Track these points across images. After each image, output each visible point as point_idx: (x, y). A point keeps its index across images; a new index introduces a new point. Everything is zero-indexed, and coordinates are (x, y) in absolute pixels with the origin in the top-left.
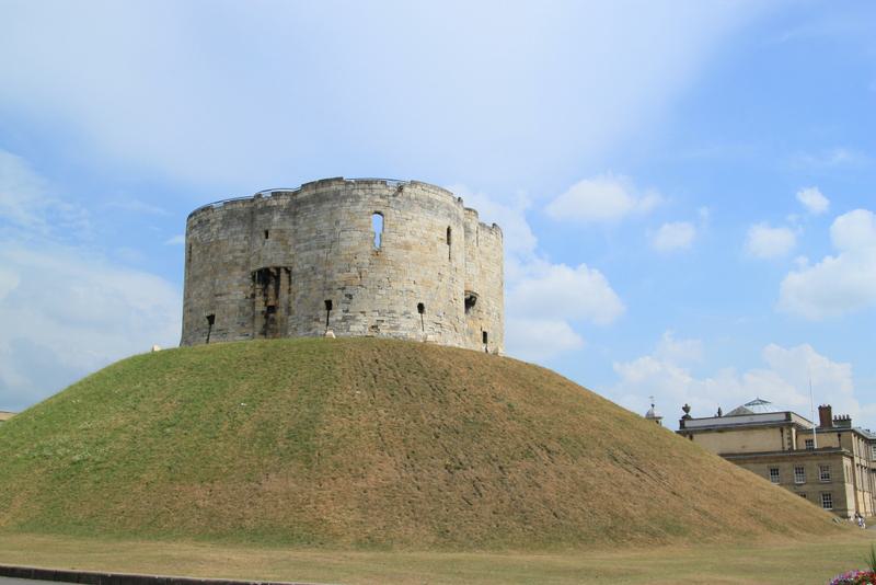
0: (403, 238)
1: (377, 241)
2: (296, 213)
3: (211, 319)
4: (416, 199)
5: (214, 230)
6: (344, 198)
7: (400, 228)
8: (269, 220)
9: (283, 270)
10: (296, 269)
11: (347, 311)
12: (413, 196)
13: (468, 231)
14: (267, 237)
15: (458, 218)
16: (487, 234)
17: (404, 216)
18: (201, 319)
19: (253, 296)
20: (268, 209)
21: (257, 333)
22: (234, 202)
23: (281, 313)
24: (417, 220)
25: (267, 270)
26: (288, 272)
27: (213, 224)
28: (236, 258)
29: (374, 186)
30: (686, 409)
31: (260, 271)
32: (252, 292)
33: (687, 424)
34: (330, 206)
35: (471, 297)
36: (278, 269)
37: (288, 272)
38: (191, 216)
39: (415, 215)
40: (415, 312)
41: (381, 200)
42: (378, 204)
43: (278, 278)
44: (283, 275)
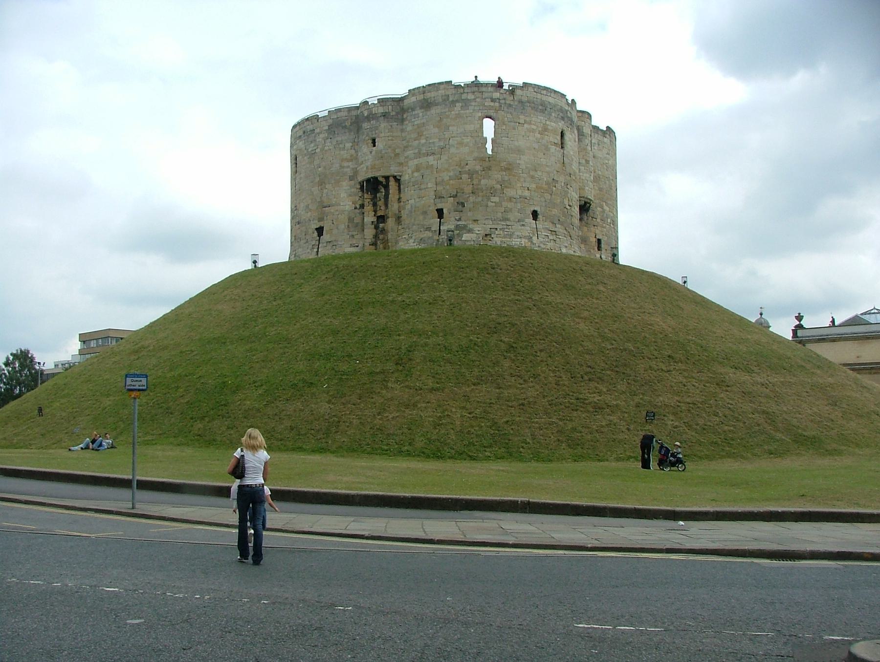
1: (489, 146)
2: (403, 121)
3: (320, 231)
4: (529, 102)
5: (319, 139)
6: (454, 102)
8: (377, 128)
9: (391, 179)
10: (405, 178)
11: (460, 220)
12: (525, 99)
13: (581, 134)
14: (374, 146)
15: (572, 121)
16: (600, 137)
18: (310, 231)
19: (362, 206)
20: (371, 117)
21: (367, 244)
22: (338, 110)
23: (391, 223)
24: (530, 124)
25: (375, 179)
27: (319, 134)
29: (484, 89)
30: (799, 318)
31: (368, 180)
32: (360, 202)
33: (800, 333)
34: (438, 111)
35: (586, 203)
36: (387, 178)
37: (397, 180)
38: (295, 127)
40: (530, 220)
41: (492, 104)
43: (386, 187)
44: (392, 183)
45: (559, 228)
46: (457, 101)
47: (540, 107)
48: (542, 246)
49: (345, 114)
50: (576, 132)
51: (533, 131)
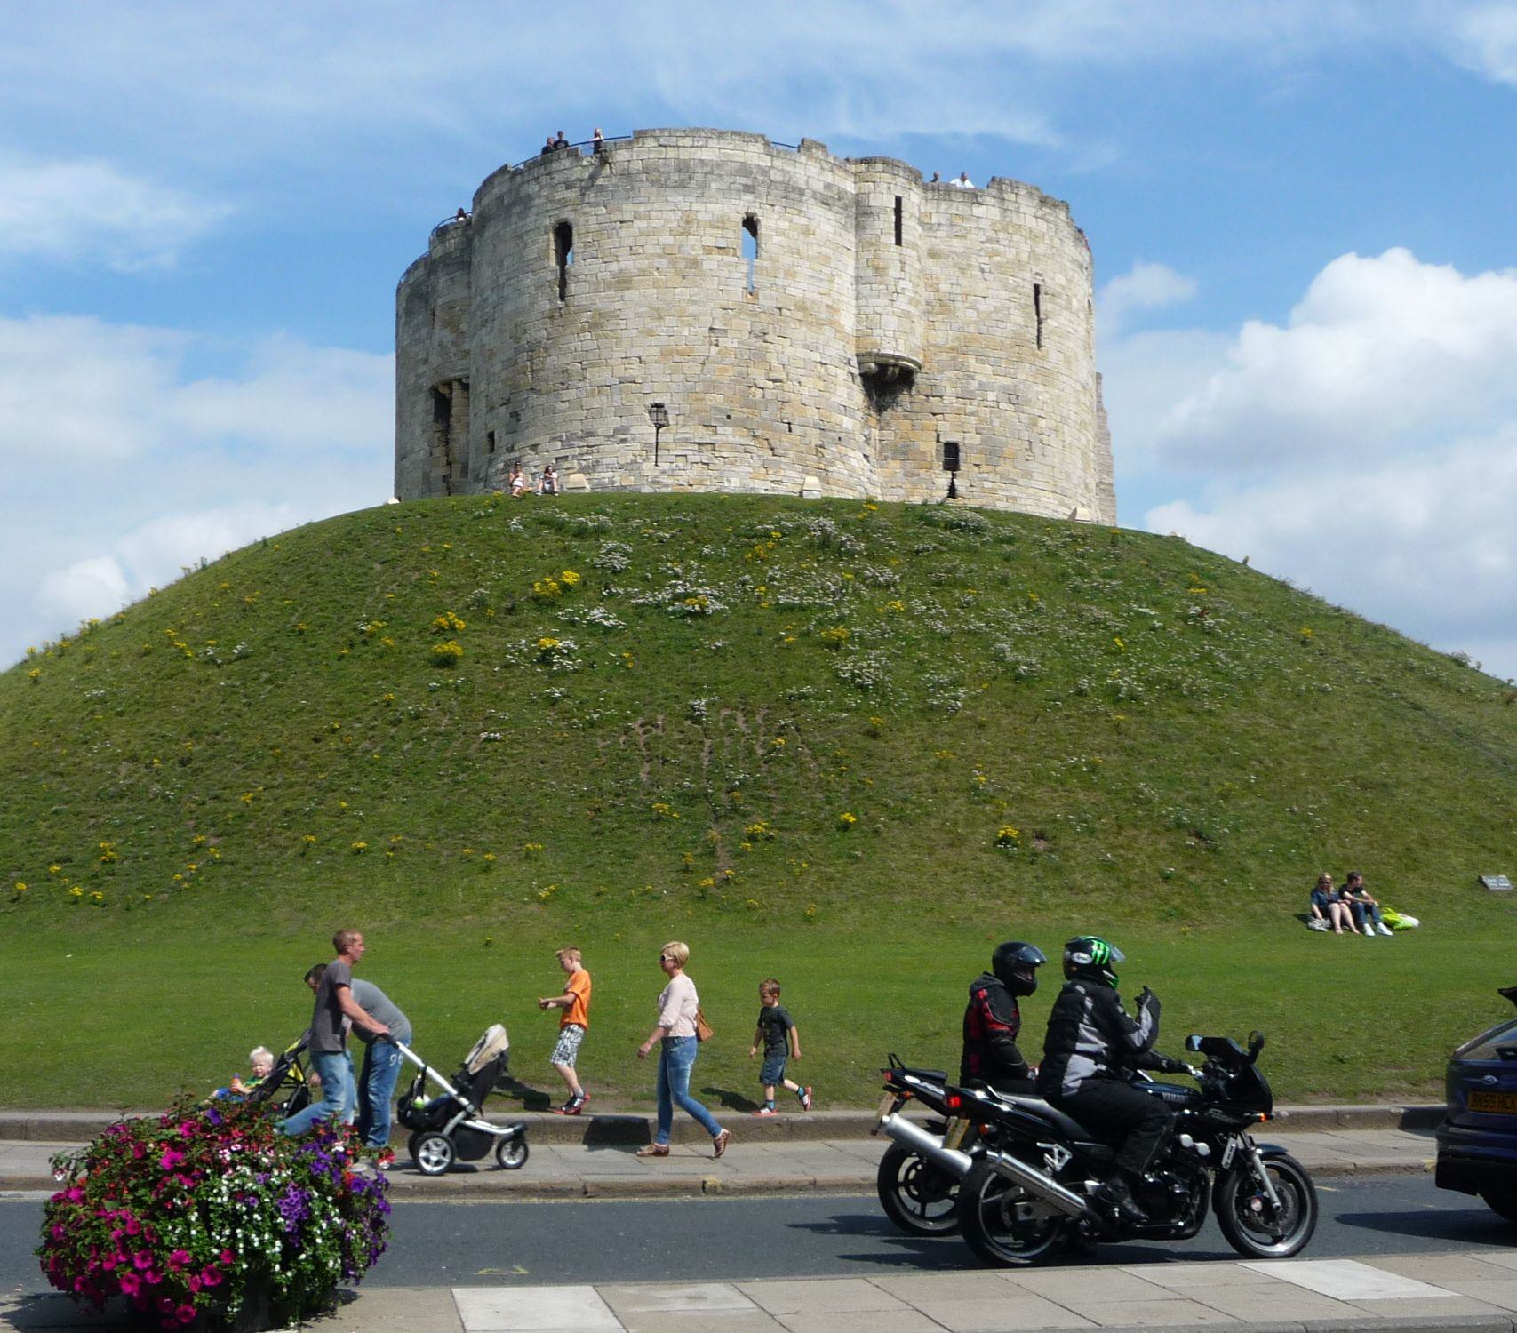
0: (614, 267)
4: (645, 171)
7: (607, 243)
9: (456, 386)
11: (511, 450)
13: (861, 212)
16: (959, 207)
17: (619, 216)
22: (415, 265)
24: (648, 218)
26: (466, 387)
28: (419, 376)
36: (449, 384)
37: (466, 387)
39: (642, 208)
41: (568, 194)
42: (563, 203)
44: (457, 393)
45: (726, 433)
46: (513, 204)
47: (675, 177)
48: (665, 480)
49: (421, 271)
50: (817, 211)
51: (654, 232)
